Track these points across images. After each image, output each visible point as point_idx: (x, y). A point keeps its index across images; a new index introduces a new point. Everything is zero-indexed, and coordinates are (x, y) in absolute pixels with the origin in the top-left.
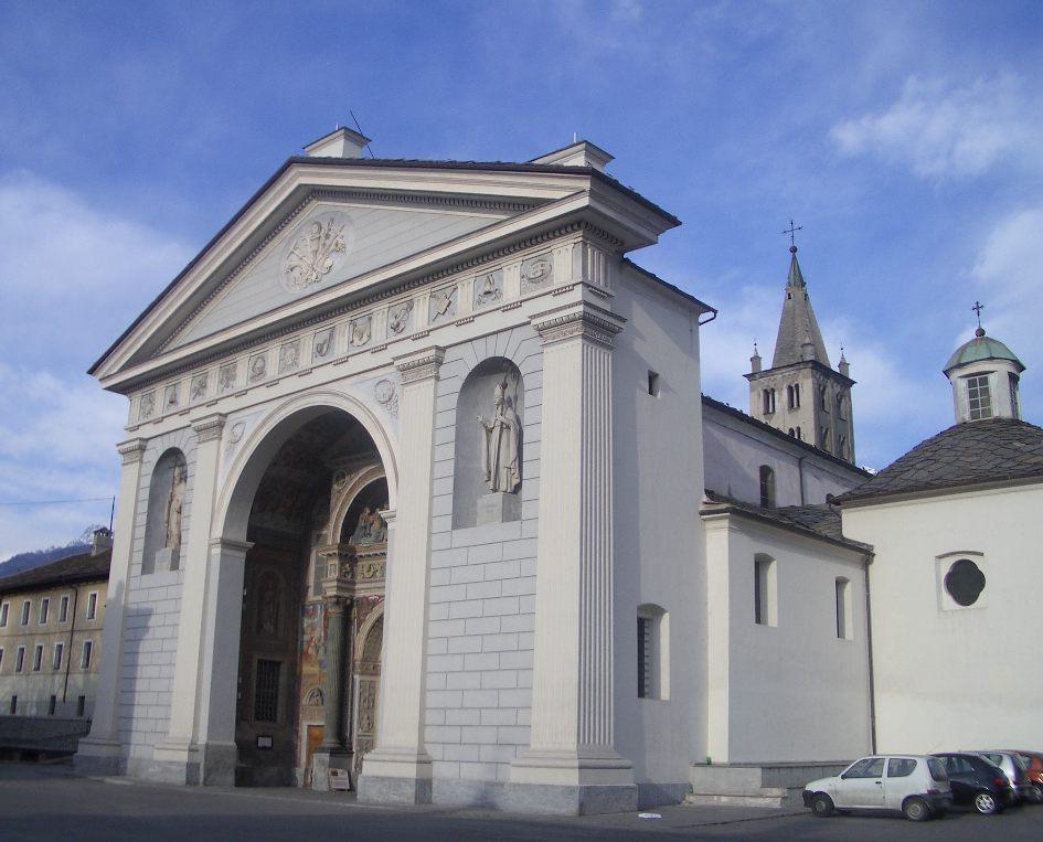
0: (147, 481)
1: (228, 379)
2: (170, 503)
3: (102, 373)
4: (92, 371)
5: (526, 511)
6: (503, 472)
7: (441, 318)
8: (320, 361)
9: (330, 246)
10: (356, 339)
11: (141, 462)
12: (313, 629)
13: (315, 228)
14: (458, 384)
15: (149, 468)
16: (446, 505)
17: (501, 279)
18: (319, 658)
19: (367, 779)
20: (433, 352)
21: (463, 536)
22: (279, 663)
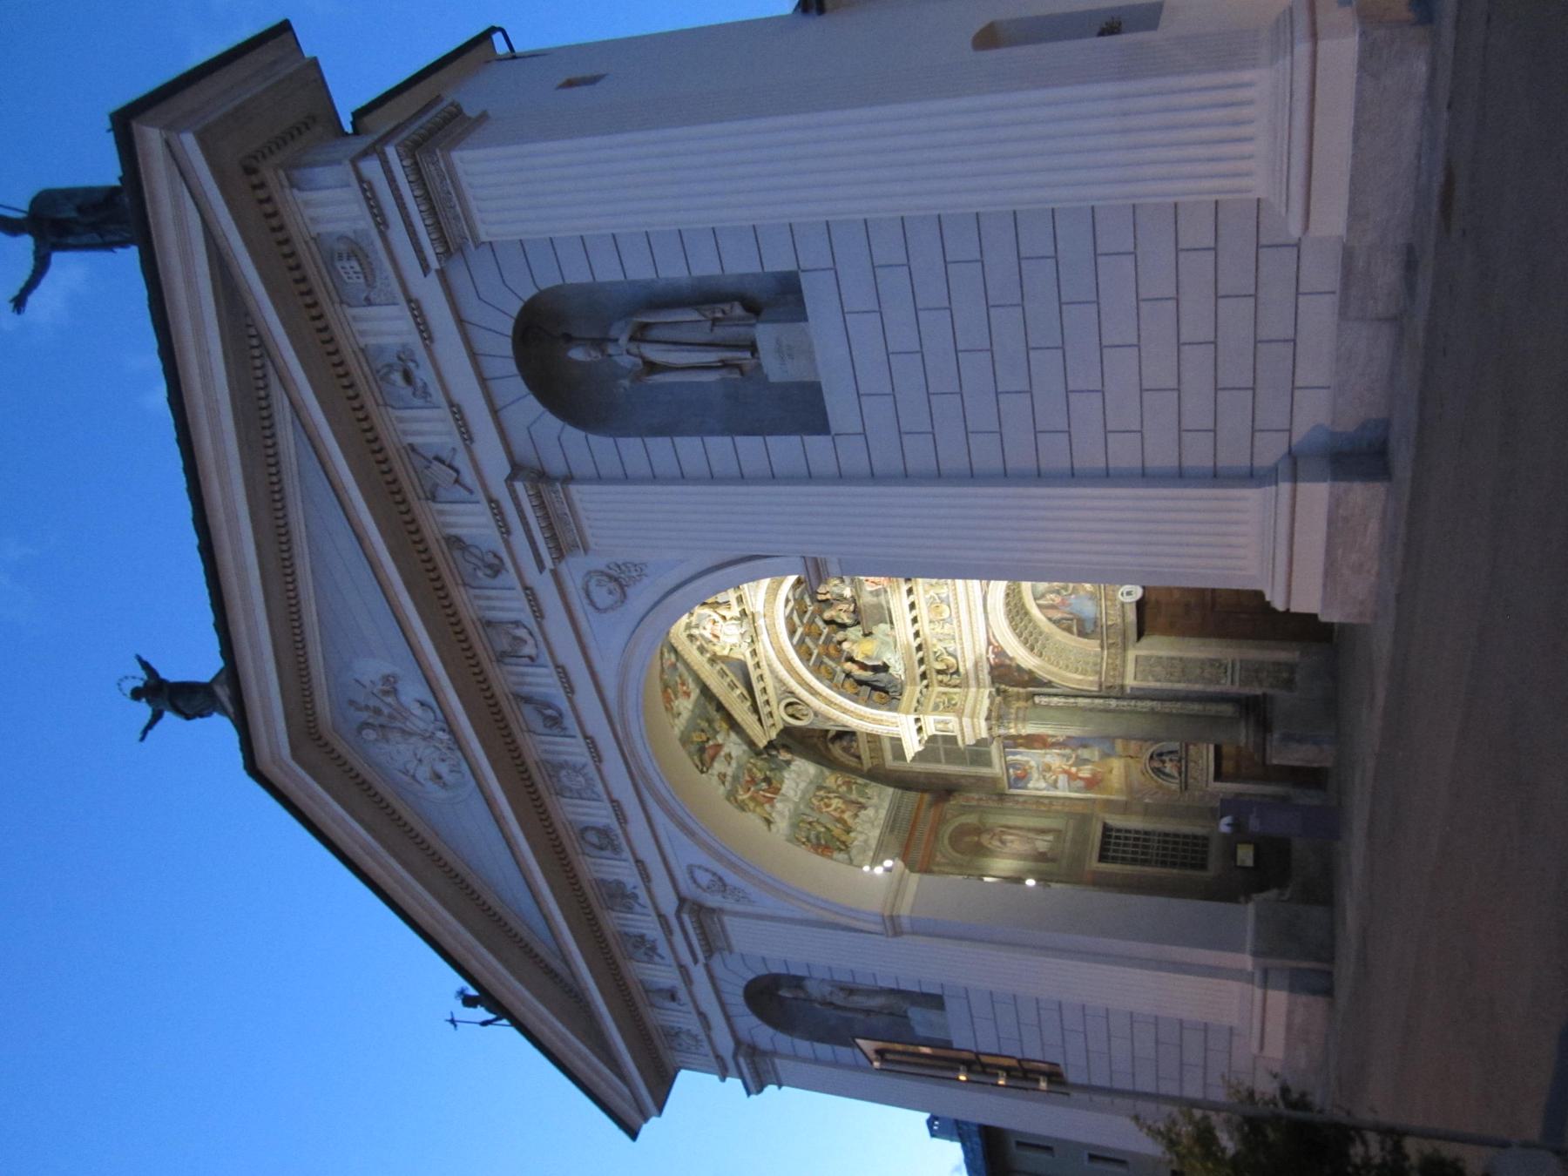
0: (803, 1046)
1: (624, 896)
2: (837, 1007)
3: (632, 1115)
4: (633, 1134)
5: (779, 262)
6: (721, 333)
7: (469, 477)
8: (569, 721)
9: (389, 705)
10: (529, 650)
11: (774, 1053)
12: (1048, 768)
13: (370, 735)
14: (552, 422)
15: (783, 1041)
16: (785, 449)
17: (381, 349)
18: (1096, 758)
19: (1326, 601)
20: (519, 486)
21: (839, 406)
22: (1107, 829)
